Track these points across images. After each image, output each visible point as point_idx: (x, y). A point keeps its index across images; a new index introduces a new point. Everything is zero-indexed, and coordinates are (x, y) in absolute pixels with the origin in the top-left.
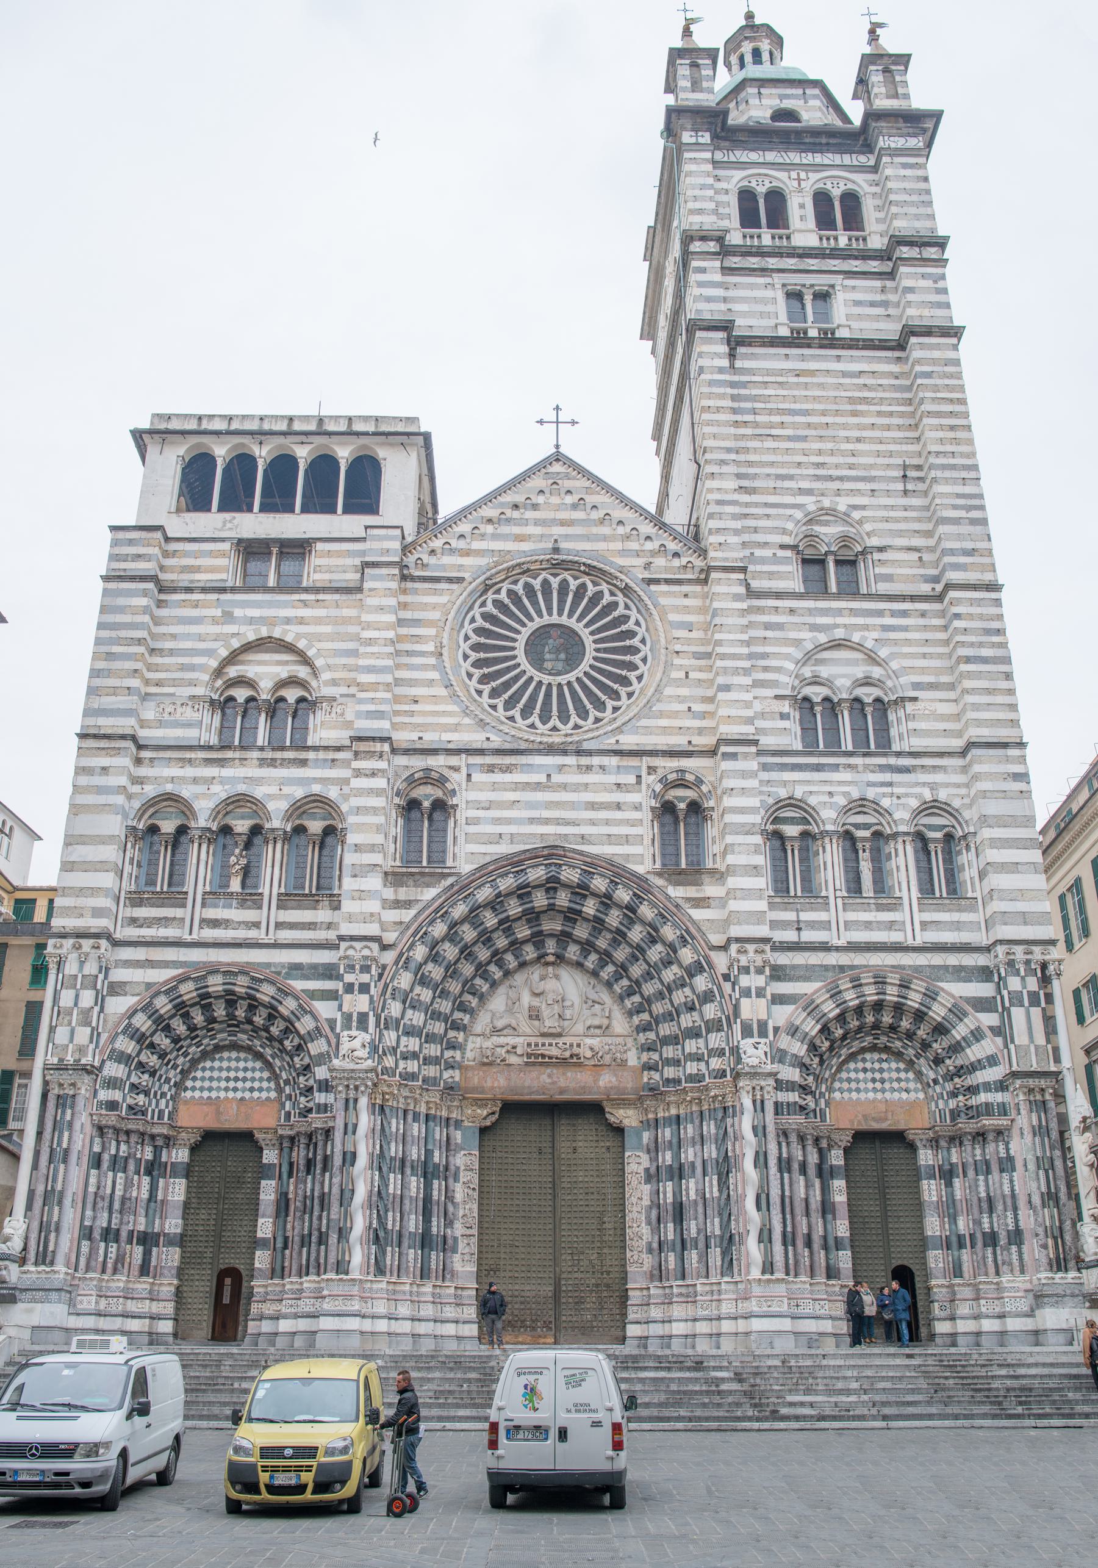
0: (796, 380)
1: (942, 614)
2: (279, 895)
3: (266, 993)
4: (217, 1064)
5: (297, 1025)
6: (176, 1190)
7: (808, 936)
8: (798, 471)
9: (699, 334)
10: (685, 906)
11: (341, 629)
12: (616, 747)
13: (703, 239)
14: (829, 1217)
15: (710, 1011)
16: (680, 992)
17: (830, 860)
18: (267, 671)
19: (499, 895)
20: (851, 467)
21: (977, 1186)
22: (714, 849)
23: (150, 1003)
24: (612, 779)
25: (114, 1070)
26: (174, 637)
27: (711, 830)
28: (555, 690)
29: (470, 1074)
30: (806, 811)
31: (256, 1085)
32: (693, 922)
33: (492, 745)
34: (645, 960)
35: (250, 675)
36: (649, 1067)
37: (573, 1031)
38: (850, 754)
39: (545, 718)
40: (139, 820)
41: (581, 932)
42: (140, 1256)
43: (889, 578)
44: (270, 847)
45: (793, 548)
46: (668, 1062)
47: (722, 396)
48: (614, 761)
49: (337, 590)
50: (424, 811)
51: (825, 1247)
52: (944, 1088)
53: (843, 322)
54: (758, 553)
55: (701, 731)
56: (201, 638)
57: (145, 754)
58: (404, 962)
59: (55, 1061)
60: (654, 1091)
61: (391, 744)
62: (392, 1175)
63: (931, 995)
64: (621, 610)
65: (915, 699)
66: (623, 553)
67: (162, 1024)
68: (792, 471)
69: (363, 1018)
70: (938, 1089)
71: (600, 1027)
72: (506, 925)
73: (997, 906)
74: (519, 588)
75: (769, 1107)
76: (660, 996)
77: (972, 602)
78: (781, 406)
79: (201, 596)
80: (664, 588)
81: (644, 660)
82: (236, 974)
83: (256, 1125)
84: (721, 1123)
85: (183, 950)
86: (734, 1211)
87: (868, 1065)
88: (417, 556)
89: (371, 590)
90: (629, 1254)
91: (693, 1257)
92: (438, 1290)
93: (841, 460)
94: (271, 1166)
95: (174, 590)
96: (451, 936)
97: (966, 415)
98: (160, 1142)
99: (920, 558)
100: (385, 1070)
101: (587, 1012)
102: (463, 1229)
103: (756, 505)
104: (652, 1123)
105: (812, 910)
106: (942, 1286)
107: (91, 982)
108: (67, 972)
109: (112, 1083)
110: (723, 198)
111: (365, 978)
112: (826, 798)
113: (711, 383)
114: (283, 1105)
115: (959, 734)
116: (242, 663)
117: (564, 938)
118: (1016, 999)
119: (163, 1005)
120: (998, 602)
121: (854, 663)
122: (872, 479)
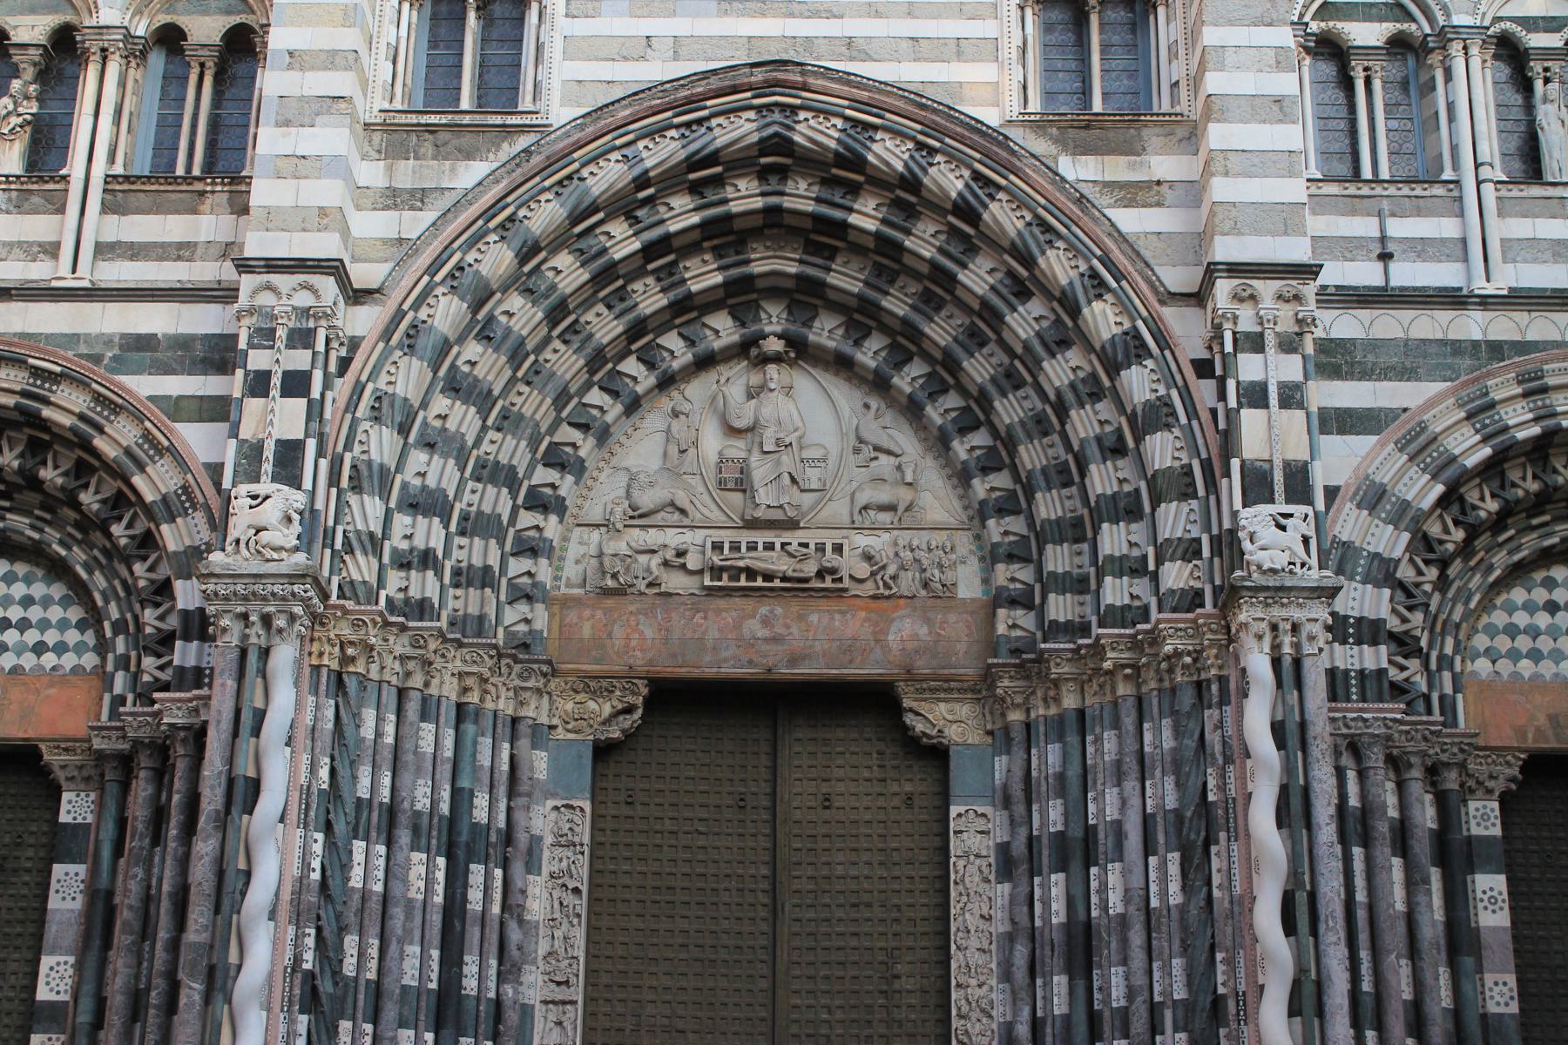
2: (110, 179)
3: (66, 406)
5: (138, 480)
7: (1406, 274)
10: (1102, 200)
14: (1468, 962)
15: (1162, 450)
19: (642, 181)
22: (1171, 70)
29: (572, 616)
31: (51, 637)
44: (92, 72)
58: (406, 334)
62: (359, 846)
69: (289, 454)
71: (891, 508)
76: (1039, 426)
83: (44, 731)
94: (78, 829)
96: (523, 280)
100: (349, 589)
104: (1018, 735)
105: (1419, 213)
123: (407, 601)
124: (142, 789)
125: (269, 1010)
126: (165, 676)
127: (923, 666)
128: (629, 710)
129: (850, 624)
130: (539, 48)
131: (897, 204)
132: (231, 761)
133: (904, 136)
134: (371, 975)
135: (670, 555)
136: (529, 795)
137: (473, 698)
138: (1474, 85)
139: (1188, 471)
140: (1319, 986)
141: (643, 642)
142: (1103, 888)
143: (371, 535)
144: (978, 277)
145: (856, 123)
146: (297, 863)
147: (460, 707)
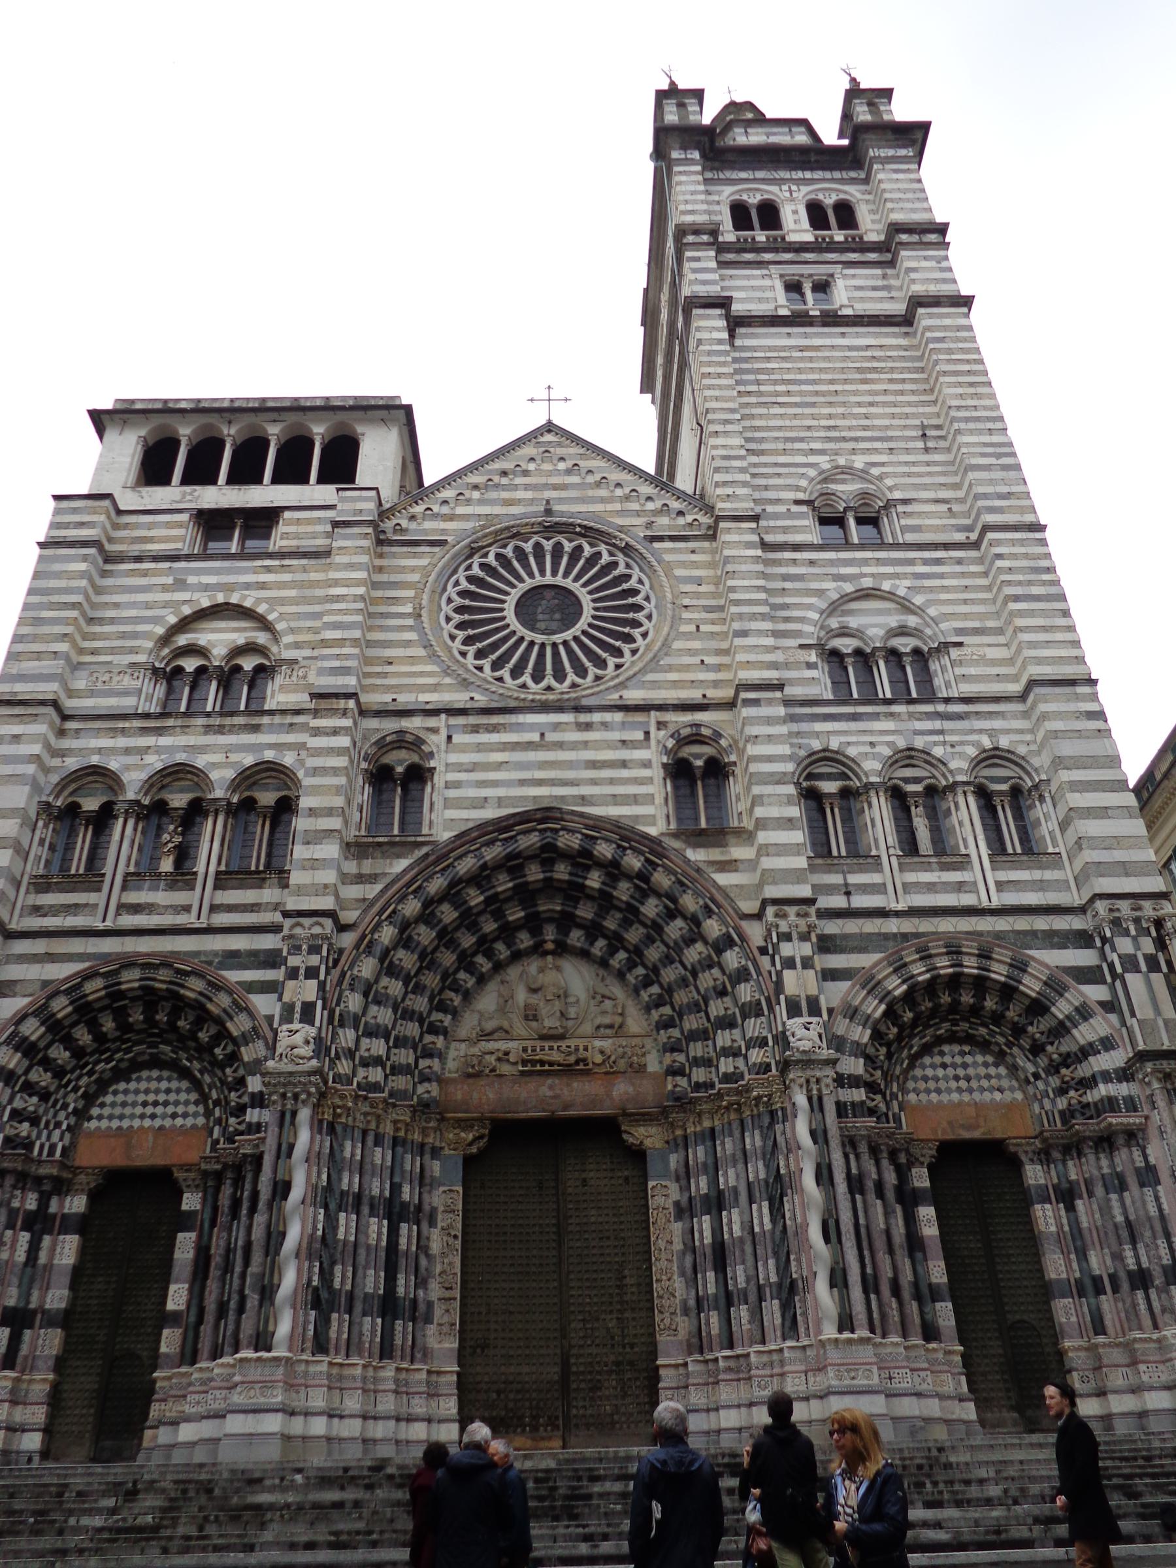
0: (799, 354)
1: (980, 561)
2: (218, 873)
4: (133, 1085)
5: (229, 1025)
6: (66, 1250)
7: (860, 901)
8: (809, 434)
9: (695, 311)
10: (709, 870)
11: (308, 592)
13: (697, 233)
14: (919, 1255)
15: (745, 993)
16: (707, 974)
17: (879, 816)
18: (219, 639)
19: (484, 867)
21: (1110, 1208)
23: (45, 1006)
24: (616, 735)
26: (116, 605)
27: (735, 787)
28: (549, 650)
29: (451, 1089)
30: (844, 764)
31: (180, 1109)
33: (476, 705)
34: (663, 942)
35: (202, 642)
36: (675, 1071)
37: (580, 1031)
38: (887, 702)
39: (538, 677)
40: (57, 797)
41: (585, 912)
46: (697, 1062)
48: (618, 717)
49: (305, 555)
51: (918, 1297)
52: (1047, 1084)
53: (846, 302)
54: (770, 509)
55: (716, 684)
56: (148, 606)
57: (71, 725)
60: (681, 1102)
61: (358, 703)
62: (342, 1215)
63: (1020, 966)
64: (621, 569)
65: (960, 644)
66: (622, 513)
67: (57, 1029)
68: (803, 434)
69: (308, 1011)
70: (1040, 1085)
71: (611, 1026)
72: (495, 905)
73: (1090, 855)
74: (509, 551)
76: (684, 983)
77: (1013, 542)
78: (786, 377)
79: (152, 565)
81: (649, 617)
82: (156, 967)
84: (768, 1132)
86: (793, 1246)
87: (948, 1059)
89: (340, 548)
91: (742, 1314)
92: (403, 1375)
93: (854, 423)
94: (191, 1214)
96: (426, 917)
97: (985, 373)
100: (338, 1078)
102: (441, 1291)
103: (765, 465)
104: (680, 1141)
105: (861, 871)
110: (717, 208)
111: (314, 960)
112: (868, 749)
113: (709, 353)
114: (211, 1133)
115: (1015, 678)
117: (566, 921)
118: (1130, 963)
119: (61, 1007)
120: (1043, 542)
121: (887, 612)
122: (891, 439)
123: (368, 1084)
124: (227, 1191)
126: (242, 1127)
130: (432, 804)
131: (608, 874)
132: (275, 1171)
134: (348, 1287)
136: (431, 1185)
137: (402, 1134)
139: (759, 1003)
140: (844, 1271)
142: (730, 1220)
143: (350, 1049)
144: (651, 908)
145: (587, 836)
146: (310, 1226)
147: (395, 1139)
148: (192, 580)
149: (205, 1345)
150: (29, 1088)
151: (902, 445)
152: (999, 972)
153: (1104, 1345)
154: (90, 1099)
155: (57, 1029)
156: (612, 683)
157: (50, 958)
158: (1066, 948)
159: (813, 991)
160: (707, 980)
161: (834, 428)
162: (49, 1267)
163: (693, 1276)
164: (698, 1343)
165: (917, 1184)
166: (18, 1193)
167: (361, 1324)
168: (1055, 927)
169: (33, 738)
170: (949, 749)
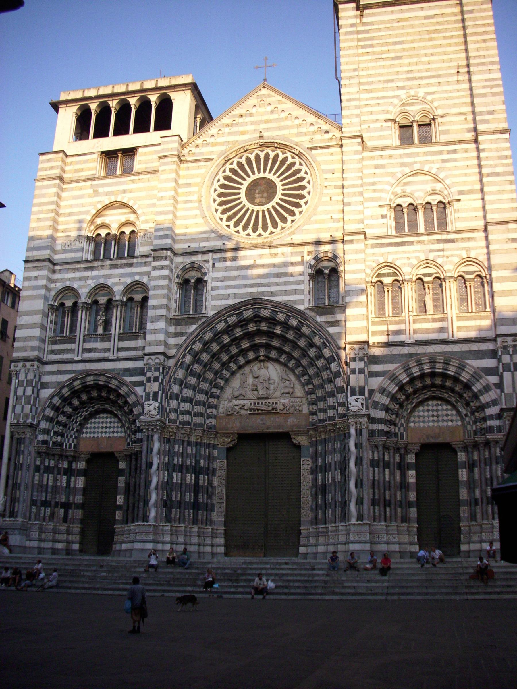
2: (119, 334)
3: (113, 384)
4: (97, 420)
6: (80, 482)
12: (291, 242)
19: (229, 326)
20: (427, 70)
23: (60, 392)
25: (44, 425)
31: (115, 430)
32: (329, 334)
38: (421, 234)
40: (55, 301)
42: (63, 514)
43: (446, 132)
45: (394, 121)
47: (352, 40)
48: (289, 249)
49: (149, 172)
50: (192, 284)
52: (471, 419)
56: (82, 205)
57: (57, 268)
59: (16, 422)
63: (461, 368)
64: (297, 166)
65: (459, 200)
66: (298, 134)
69: (155, 394)
70: (467, 419)
71: (288, 393)
74: (243, 161)
75: (365, 432)
78: (388, 41)
80: (319, 151)
85: (74, 365)
86: (347, 489)
87: (430, 408)
88: (189, 149)
89: (163, 171)
90: (302, 511)
91: (329, 512)
94: (123, 470)
95: (70, 182)
98: (70, 459)
99: (466, 119)
101: (281, 386)
103: (372, 99)
106: (466, 526)
107: (29, 383)
108: (20, 379)
109: (46, 432)
111: (157, 374)
112: (406, 261)
116: (102, 216)
118: (506, 368)
121: (426, 182)
125: (157, 507)
127: (295, 429)
128: (234, 440)
129: (279, 420)
132: (147, 458)
133: (284, 313)
134: (179, 499)
135: (241, 406)
137: (199, 441)
138: (409, 293)
139: (343, 387)
140: (362, 498)
141: (235, 426)
148: (101, 190)
149: (130, 519)
150: (59, 423)
151: (446, 79)
152: (451, 371)
153: (473, 525)
154: (82, 425)
155: (66, 401)
156: (288, 232)
157: (59, 372)
158: (484, 359)
159: (362, 383)
160: (325, 375)
161: (411, 71)
162: (75, 488)
163: (315, 496)
164: (315, 521)
165: (409, 461)
166: (60, 462)
167: (184, 512)
168: (481, 349)
169: (42, 277)
170: (445, 259)
